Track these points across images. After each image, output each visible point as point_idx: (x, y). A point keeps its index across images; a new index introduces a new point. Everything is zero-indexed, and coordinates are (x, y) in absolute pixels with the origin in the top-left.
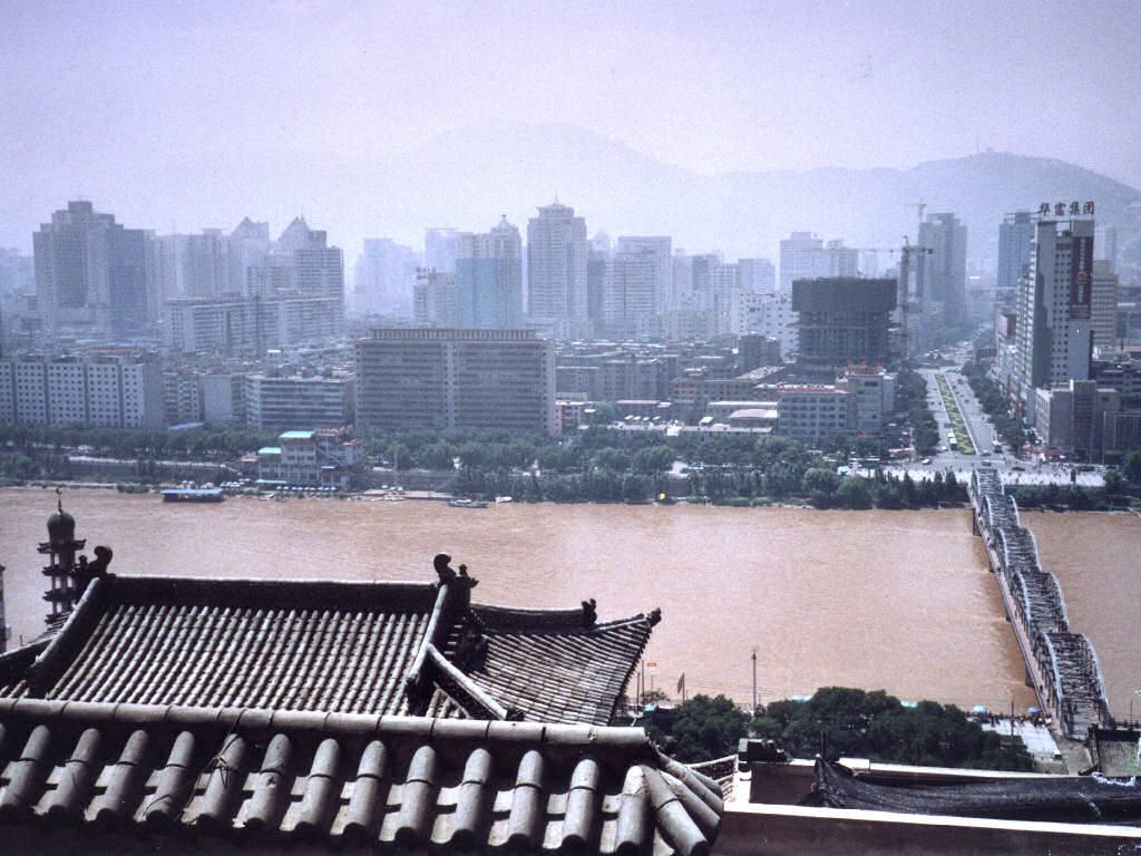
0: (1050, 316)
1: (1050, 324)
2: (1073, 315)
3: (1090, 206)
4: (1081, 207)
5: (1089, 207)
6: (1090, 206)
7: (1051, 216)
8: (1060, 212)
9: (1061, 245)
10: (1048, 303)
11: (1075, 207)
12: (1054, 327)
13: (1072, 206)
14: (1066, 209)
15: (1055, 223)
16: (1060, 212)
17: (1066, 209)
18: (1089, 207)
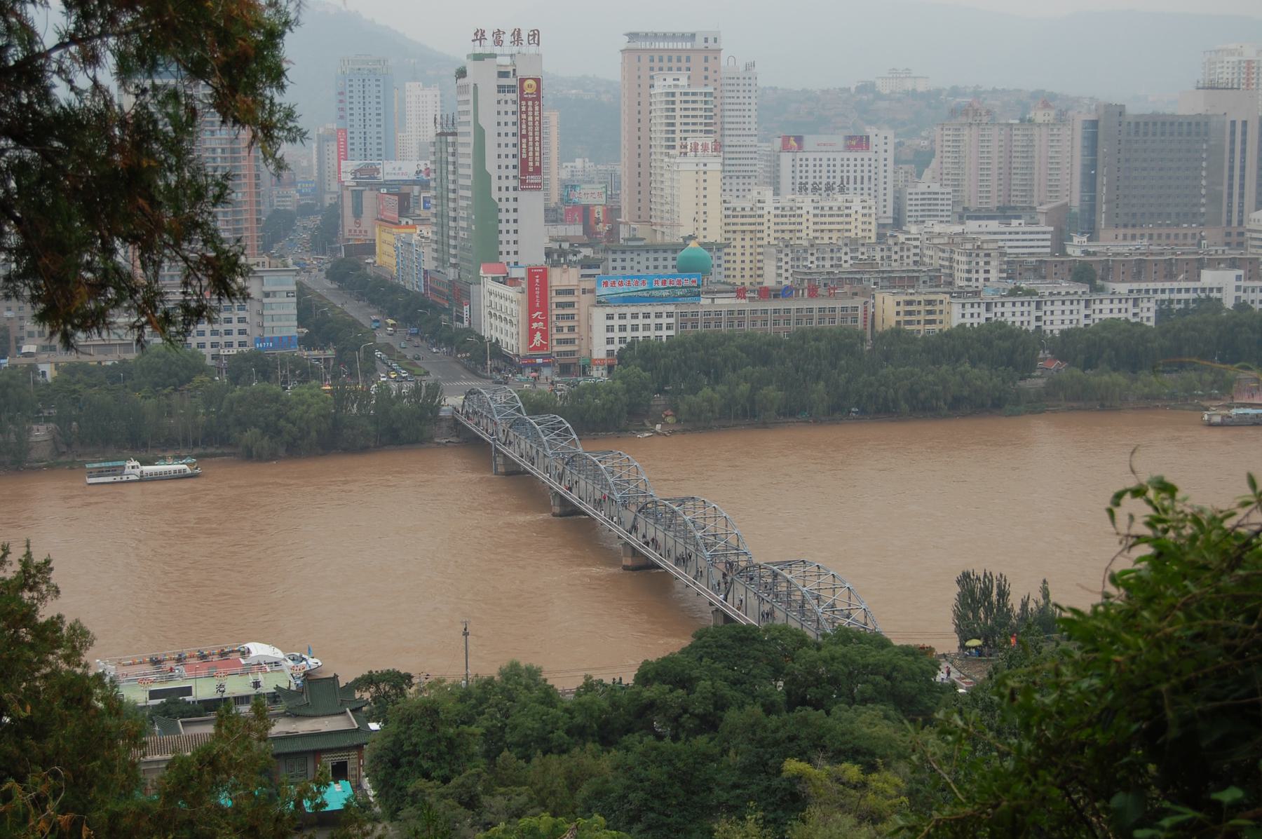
0: (495, 184)
1: (495, 195)
2: (524, 185)
3: (535, 35)
4: (524, 36)
5: (534, 35)
6: (535, 35)
7: (488, 46)
8: (498, 42)
9: (504, 86)
10: (491, 166)
11: (517, 34)
12: (500, 200)
13: (513, 34)
14: (507, 38)
15: (494, 56)
16: (498, 42)
17: (507, 38)
18: (534, 35)
